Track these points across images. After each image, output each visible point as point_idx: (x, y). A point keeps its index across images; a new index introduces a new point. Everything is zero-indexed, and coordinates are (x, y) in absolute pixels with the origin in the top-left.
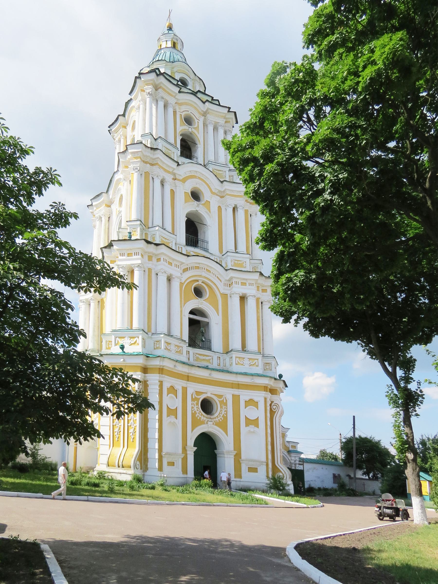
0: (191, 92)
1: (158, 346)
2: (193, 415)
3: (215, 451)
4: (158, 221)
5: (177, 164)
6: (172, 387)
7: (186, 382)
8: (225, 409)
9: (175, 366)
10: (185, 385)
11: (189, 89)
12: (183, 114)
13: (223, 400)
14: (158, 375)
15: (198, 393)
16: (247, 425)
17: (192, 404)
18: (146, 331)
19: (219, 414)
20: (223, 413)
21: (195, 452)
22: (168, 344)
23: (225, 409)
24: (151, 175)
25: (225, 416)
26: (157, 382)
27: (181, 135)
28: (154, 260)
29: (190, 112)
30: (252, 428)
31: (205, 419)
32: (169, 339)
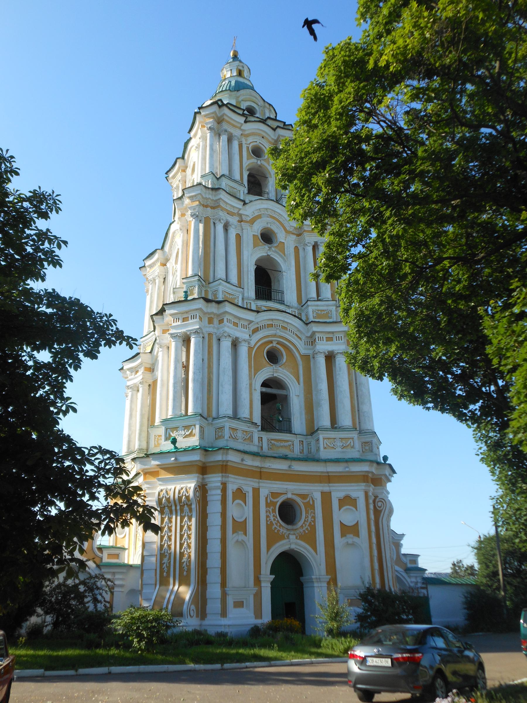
0: (259, 120)
1: (220, 434)
2: (269, 526)
3: (301, 578)
4: (221, 273)
5: (242, 203)
6: (239, 490)
7: (257, 480)
8: (312, 515)
9: (242, 460)
10: (256, 485)
11: (257, 117)
12: (250, 146)
13: (309, 501)
14: (220, 475)
15: (275, 495)
16: (343, 535)
17: (267, 512)
18: (205, 415)
19: (304, 523)
20: (310, 520)
21: (272, 583)
22: (234, 429)
23: (312, 515)
24: (212, 221)
25: (313, 524)
26: (219, 484)
27: (248, 170)
28: (216, 321)
29: (258, 142)
30: (351, 539)
31: (285, 531)
32: (235, 424)
